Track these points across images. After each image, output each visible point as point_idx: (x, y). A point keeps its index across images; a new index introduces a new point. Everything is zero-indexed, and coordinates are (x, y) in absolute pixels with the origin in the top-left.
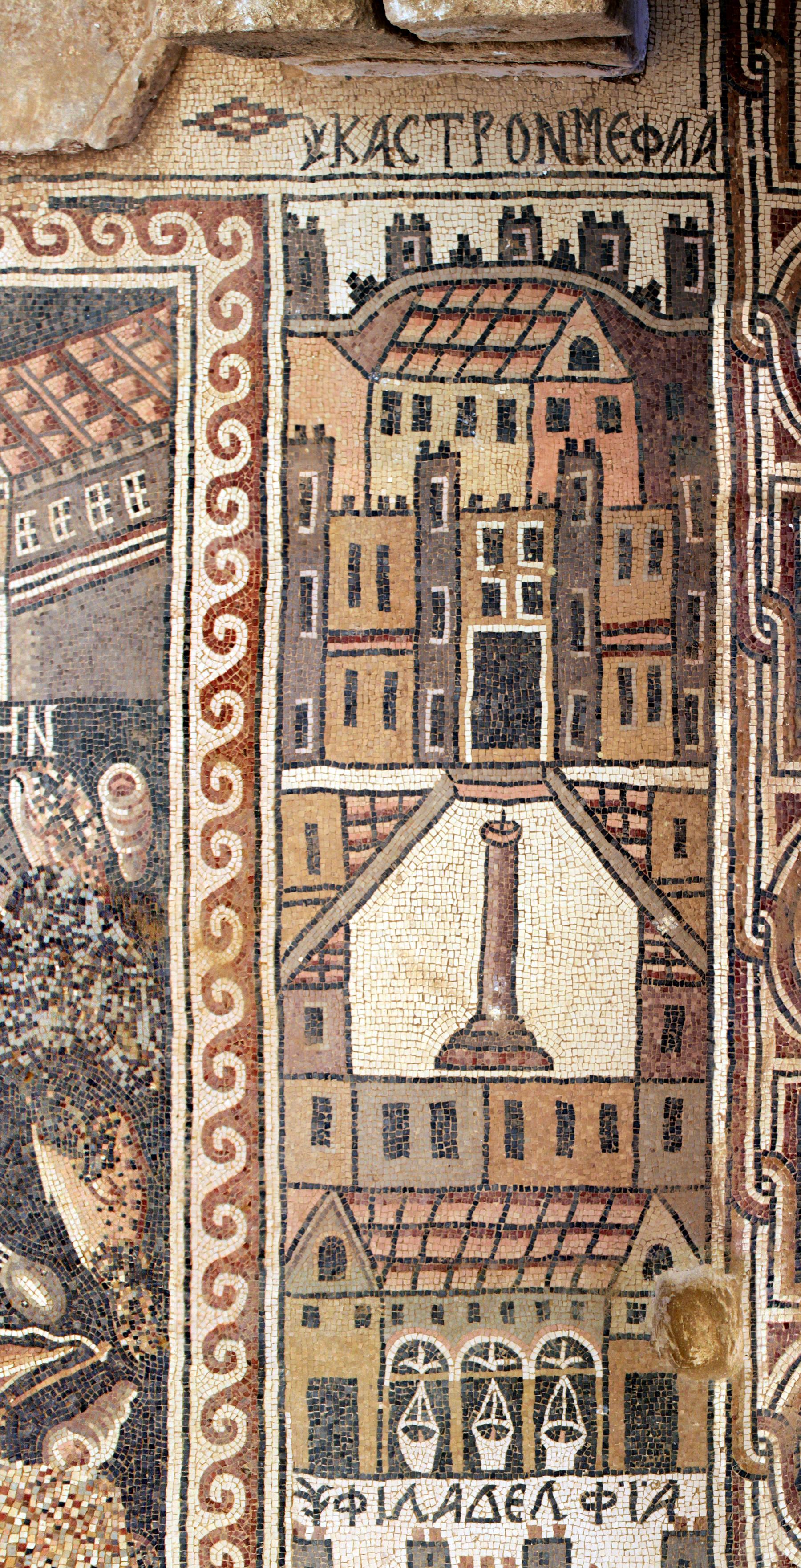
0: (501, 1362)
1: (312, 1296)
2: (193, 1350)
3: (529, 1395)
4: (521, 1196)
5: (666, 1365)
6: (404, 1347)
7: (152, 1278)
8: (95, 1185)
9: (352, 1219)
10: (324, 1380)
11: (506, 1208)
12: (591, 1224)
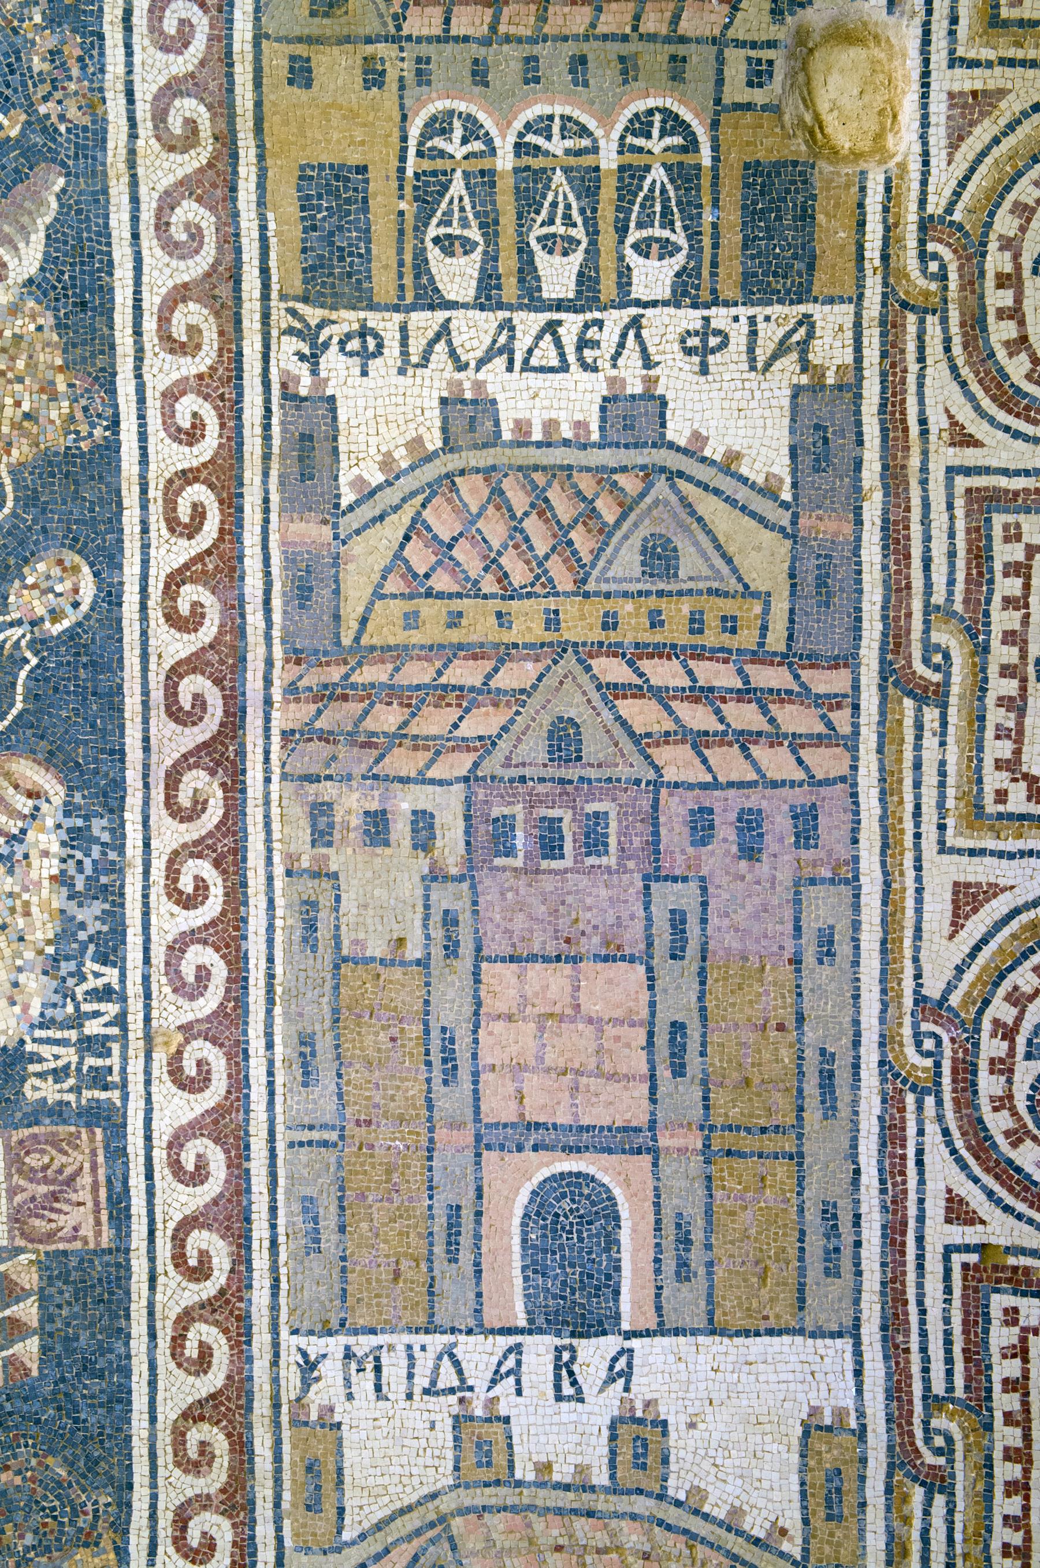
0: (569, 143)
3: (608, 193)
5: (799, 147)
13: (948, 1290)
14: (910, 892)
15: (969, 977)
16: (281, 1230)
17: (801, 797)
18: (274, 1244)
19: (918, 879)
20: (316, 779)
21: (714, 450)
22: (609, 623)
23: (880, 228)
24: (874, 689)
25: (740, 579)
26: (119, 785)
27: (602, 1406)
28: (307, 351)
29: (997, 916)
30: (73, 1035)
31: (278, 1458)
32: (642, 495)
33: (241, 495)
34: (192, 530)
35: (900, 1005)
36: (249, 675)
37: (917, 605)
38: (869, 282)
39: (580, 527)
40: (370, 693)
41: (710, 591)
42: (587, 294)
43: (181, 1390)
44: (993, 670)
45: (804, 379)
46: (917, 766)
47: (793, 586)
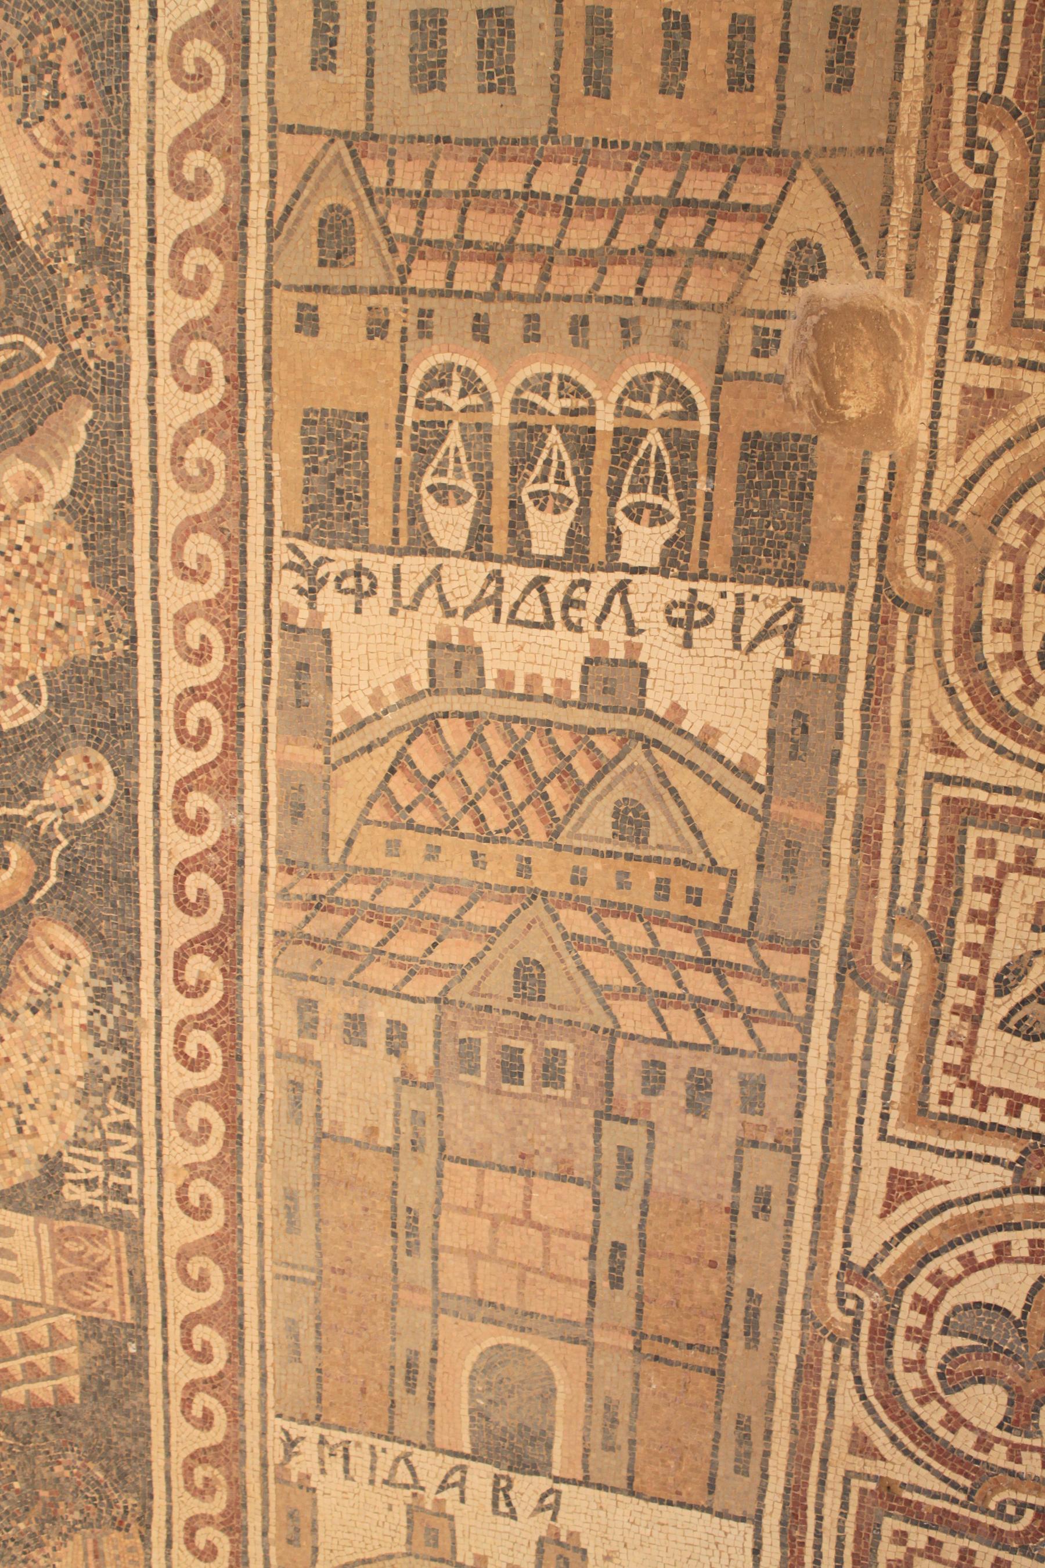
0: (567, 403)
1: (309, 289)
2: (159, 356)
3: (603, 454)
4: (603, 154)
6: (433, 371)
7: (107, 259)
8: (36, 132)
9: (364, 180)
10: (324, 412)
11: (581, 173)
12: (706, 203)
13: (845, 1505)
14: (848, 1170)
15: (896, 1253)
16: (269, 1339)
17: (749, 1066)
18: (262, 1348)
19: (857, 1160)
20: (304, 978)
21: (692, 724)
22: (578, 878)
23: (879, 517)
24: (831, 979)
25: (708, 854)
26: (135, 958)
27: (532, 1526)
28: (306, 586)
29: (929, 1206)
30: (100, 1155)
31: (266, 1503)
32: (618, 759)
33: (242, 715)
34: (198, 743)
35: (827, 1266)
36: (247, 878)
37: (883, 905)
38: (862, 573)
39: (555, 782)
40: (353, 910)
41: (678, 862)
42: (575, 555)
43: (188, 1438)
44: (952, 978)
45: (788, 665)
46: (867, 1057)
47: (760, 867)
